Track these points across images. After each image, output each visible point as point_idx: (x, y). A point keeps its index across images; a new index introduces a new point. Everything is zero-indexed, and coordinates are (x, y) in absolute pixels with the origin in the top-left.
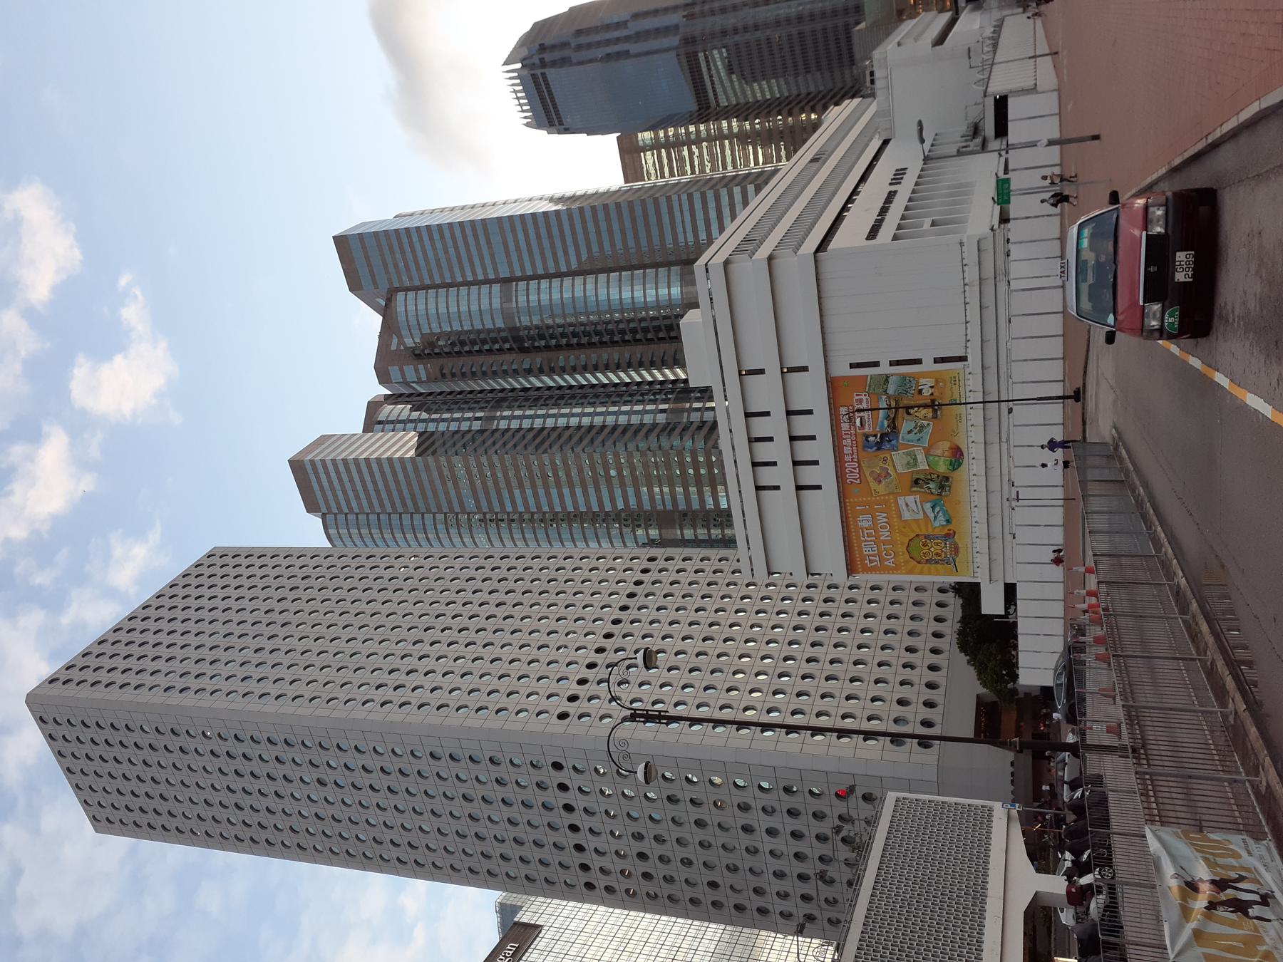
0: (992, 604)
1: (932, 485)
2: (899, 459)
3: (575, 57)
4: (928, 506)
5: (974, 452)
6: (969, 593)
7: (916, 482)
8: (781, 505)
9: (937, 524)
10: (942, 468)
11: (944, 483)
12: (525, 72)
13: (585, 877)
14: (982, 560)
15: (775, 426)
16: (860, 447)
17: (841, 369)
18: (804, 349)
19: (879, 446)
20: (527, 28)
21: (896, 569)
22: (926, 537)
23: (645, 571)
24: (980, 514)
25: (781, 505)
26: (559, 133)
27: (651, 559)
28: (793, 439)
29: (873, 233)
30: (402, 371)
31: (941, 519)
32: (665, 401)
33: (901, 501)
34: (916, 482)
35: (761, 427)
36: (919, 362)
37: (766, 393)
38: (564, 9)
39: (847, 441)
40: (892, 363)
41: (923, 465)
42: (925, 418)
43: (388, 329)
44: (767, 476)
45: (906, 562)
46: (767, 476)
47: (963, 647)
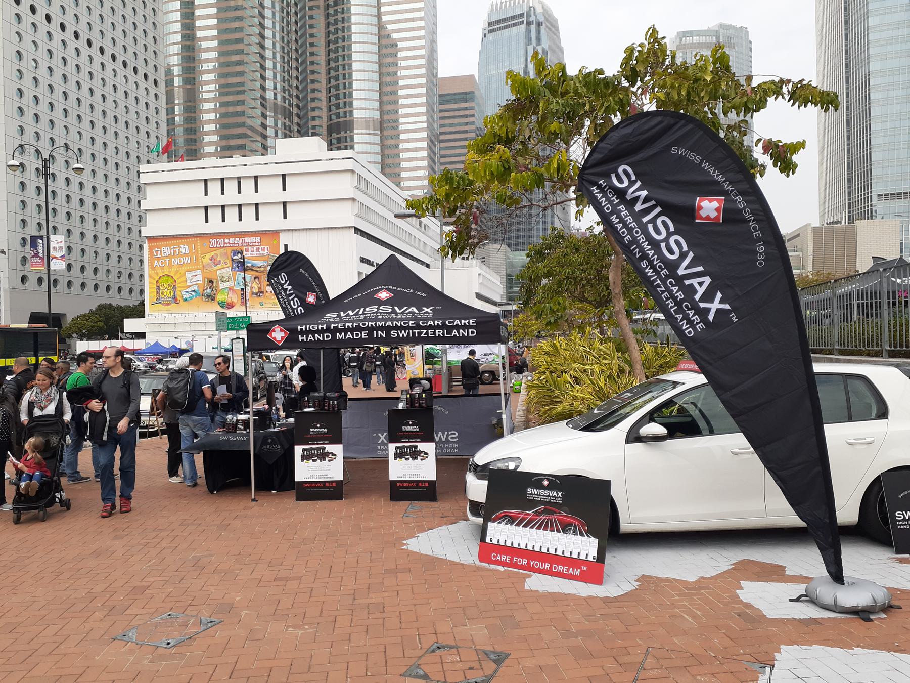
0: (131, 325)
1: (209, 291)
2: (227, 271)
4: (196, 289)
6: (138, 312)
9: (183, 293)
10: (220, 297)
11: (211, 298)
14: (160, 319)
15: (248, 195)
16: (235, 249)
17: (284, 239)
21: (152, 267)
23: (146, 76)
24: (190, 318)
27: (156, 82)
29: (363, 260)
31: (187, 296)
32: (284, 99)
34: (211, 282)
35: (248, 186)
37: (270, 191)
38: (564, 43)
39: (237, 241)
41: (221, 286)
42: (252, 288)
44: (214, 187)
45: (157, 274)
46: (214, 187)
47: (101, 307)
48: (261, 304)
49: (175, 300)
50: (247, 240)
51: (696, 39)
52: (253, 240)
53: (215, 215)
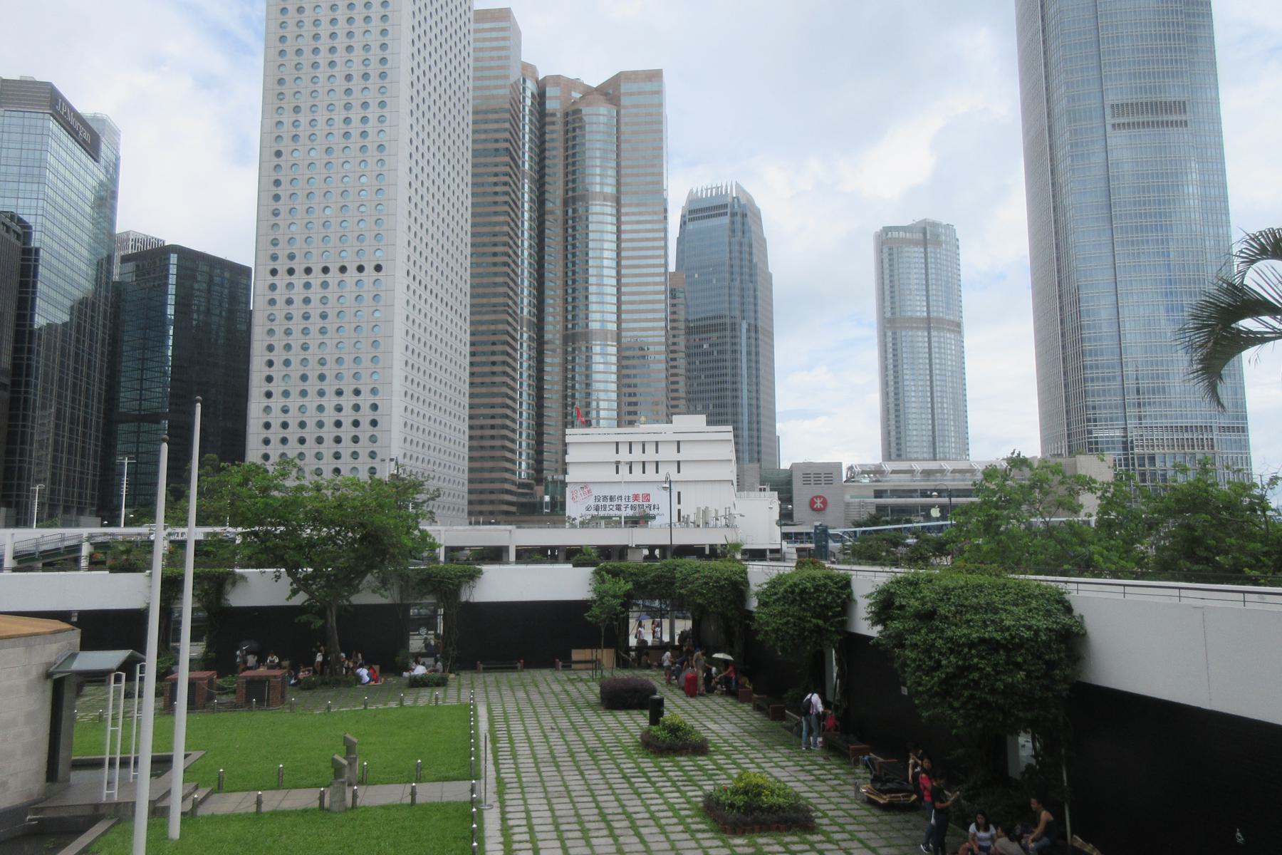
3: (737, 239)
8: (609, 454)
12: (730, 200)
13: (282, 270)
15: (650, 455)
20: (759, 202)
25: (609, 454)
26: (683, 216)
28: (644, 463)
30: (556, 98)
35: (650, 449)
37: (667, 453)
38: (766, 234)
43: (588, 92)
44: (624, 449)
46: (624, 449)
51: (902, 234)
53: (624, 469)
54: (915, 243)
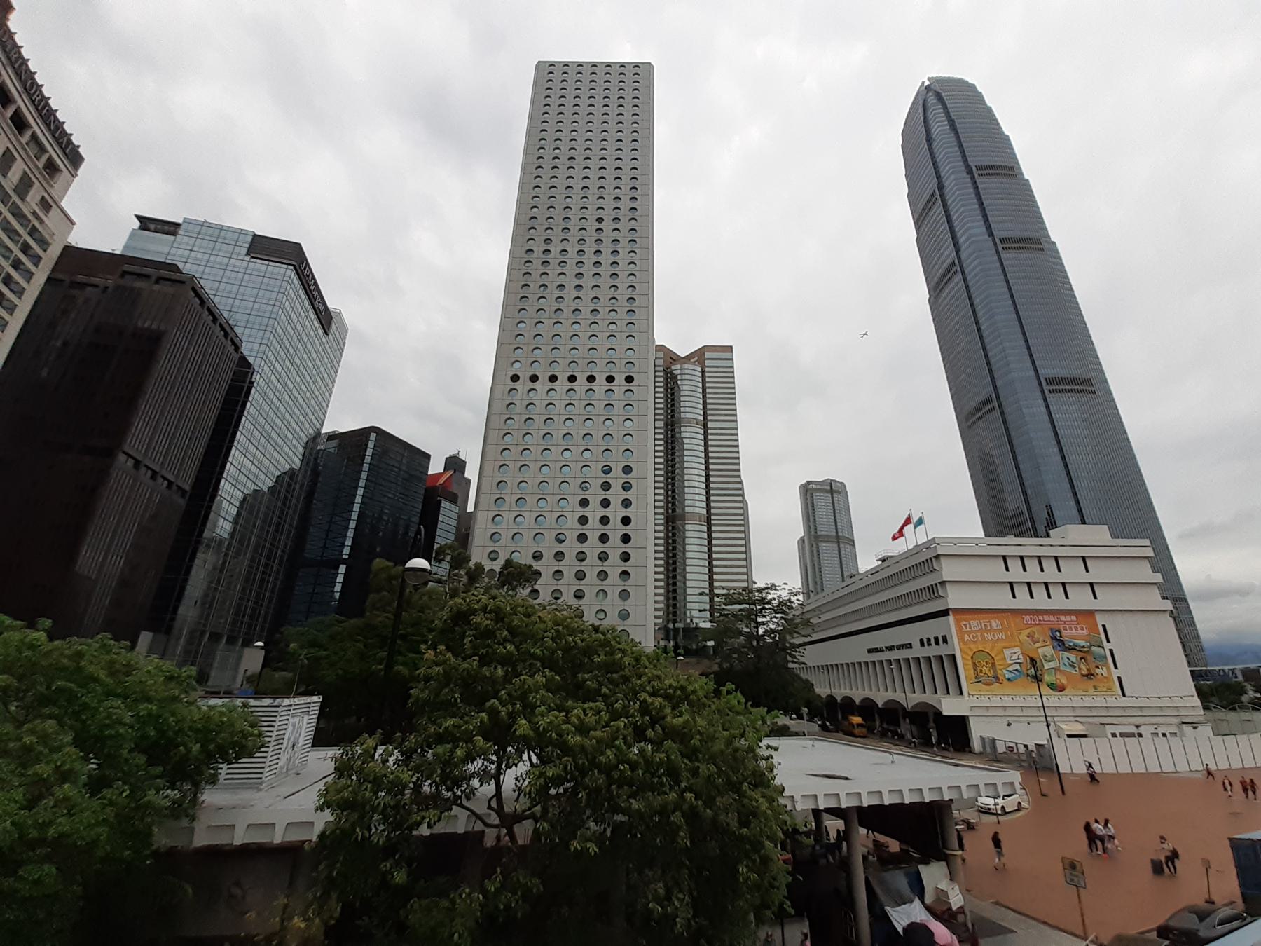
2: (1048, 650)
4: (1018, 667)
5: (1063, 700)
7: (1033, 661)
10: (1047, 678)
13: (524, 377)
14: (984, 701)
17: (1100, 620)
18: (1107, 599)
19: (1054, 638)
22: (993, 665)
24: (1019, 701)
25: (995, 571)
31: (1009, 675)
33: (1016, 650)
34: (1033, 661)
36: (1116, 667)
39: (1052, 618)
40: (1111, 651)
41: (1047, 666)
44: (1015, 565)
48: (1095, 687)
49: (997, 679)
50: (1063, 618)
52: (1068, 618)
53: (1022, 592)
54: (826, 491)
